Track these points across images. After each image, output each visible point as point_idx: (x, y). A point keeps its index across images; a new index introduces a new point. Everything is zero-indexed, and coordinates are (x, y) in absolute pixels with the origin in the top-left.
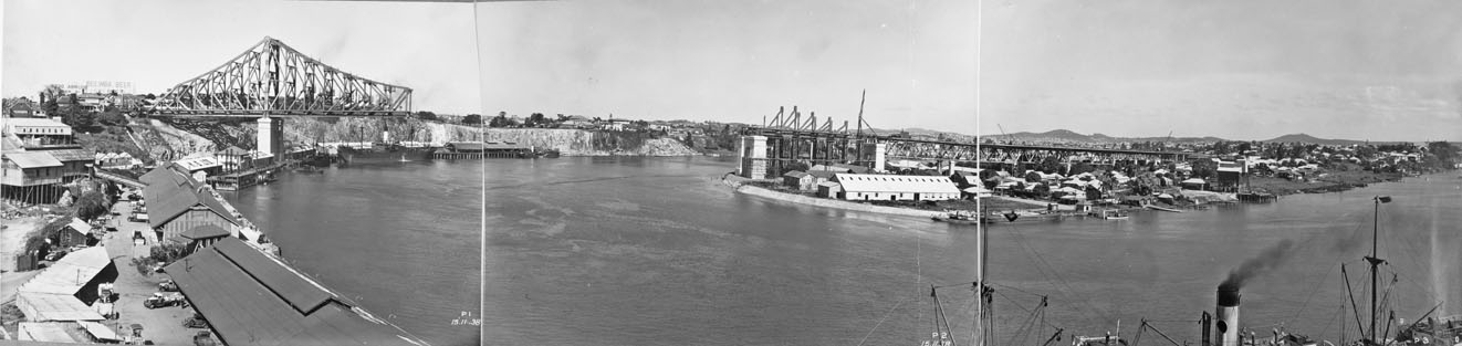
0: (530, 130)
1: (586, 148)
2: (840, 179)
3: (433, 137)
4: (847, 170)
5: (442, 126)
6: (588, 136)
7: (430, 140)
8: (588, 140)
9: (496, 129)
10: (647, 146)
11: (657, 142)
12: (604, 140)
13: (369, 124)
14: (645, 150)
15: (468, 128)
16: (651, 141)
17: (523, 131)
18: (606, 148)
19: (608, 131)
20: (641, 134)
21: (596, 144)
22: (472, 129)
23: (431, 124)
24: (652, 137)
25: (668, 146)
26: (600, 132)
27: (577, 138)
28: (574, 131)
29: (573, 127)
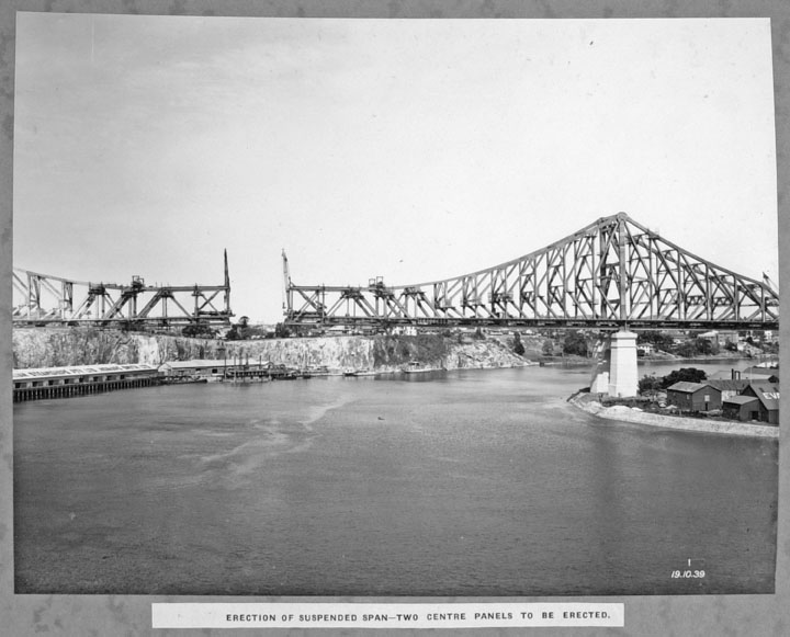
1: (365, 363)
2: (757, 392)
3: (141, 357)
4: (768, 377)
5: (153, 339)
6: (367, 345)
7: (136, 361)
8: (366, 353)
9: (236, 342)
10: (454, 356)
11: (470, 349)
13: (38, 340)
14: (451, 363)
16: (460, 349)
17: (274, 342)
18: (394, 361)
19: (396, 336)
20: (446, 339)
21: (379, 359)
24: (461, 342)
25: (486, 354)
26: (387, 338)
27: (351, 348)
28: (345, 340)
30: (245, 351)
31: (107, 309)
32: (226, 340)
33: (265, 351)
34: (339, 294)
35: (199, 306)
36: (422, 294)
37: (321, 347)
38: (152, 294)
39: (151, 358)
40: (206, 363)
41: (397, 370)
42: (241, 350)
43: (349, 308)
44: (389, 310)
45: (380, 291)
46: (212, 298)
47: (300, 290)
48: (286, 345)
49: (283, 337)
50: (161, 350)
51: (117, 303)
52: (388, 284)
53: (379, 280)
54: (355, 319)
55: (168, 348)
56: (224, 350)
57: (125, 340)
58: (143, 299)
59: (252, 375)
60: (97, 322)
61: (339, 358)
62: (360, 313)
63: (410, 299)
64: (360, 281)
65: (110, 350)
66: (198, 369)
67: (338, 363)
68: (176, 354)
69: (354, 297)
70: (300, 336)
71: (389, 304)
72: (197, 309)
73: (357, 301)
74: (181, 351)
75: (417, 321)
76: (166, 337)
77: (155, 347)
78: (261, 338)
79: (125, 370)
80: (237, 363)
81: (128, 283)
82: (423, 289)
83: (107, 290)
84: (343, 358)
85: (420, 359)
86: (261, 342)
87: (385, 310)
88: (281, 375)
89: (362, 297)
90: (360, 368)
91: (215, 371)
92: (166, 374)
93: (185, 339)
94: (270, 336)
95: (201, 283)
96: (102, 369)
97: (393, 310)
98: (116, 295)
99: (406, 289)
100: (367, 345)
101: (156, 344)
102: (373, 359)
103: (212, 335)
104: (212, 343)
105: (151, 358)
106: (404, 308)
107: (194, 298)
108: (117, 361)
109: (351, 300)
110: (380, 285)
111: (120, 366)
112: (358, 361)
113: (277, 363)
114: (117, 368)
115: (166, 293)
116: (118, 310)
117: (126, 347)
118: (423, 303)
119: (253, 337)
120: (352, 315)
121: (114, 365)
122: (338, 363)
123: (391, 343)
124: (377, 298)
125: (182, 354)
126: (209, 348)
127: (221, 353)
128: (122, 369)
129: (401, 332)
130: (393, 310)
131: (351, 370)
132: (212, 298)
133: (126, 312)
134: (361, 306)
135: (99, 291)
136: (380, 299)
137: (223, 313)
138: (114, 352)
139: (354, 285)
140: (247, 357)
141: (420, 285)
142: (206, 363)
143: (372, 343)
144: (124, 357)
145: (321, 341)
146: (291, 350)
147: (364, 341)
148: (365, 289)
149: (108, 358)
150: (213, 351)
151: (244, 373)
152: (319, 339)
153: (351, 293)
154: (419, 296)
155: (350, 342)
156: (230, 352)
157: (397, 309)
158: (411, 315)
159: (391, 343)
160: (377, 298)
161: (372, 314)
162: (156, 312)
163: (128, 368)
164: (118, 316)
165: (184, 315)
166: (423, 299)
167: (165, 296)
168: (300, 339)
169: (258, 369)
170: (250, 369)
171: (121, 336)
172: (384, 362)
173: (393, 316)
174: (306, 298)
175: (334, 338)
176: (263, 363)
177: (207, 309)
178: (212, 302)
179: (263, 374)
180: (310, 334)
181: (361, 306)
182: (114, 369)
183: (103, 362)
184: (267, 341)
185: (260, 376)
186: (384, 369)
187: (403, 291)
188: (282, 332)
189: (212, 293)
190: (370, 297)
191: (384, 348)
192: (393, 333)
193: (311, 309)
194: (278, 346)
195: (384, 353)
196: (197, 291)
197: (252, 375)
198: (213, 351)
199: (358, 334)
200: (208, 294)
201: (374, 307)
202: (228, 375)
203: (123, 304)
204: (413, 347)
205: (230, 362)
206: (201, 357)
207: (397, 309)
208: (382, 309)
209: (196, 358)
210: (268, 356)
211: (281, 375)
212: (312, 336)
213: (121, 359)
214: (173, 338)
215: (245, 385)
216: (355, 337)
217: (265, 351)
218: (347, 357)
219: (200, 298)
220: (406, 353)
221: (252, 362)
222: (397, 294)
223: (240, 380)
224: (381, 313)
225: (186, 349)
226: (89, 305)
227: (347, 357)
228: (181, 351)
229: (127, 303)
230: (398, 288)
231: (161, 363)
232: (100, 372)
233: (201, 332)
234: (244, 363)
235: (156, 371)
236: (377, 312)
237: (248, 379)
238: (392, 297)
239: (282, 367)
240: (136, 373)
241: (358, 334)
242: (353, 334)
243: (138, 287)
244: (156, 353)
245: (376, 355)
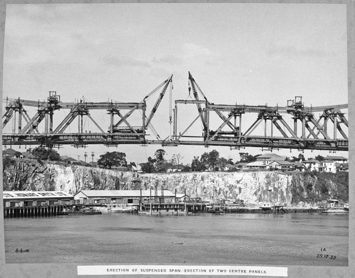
0: (199, 175)
1: (283, 199)
3: (57, 185)
5: (69, 169)
6: (285, 180)
7: (52, 189)
8: (284, 190)
9: (151, 175)
12: (309, 187)
15: (107, 172)
17: (190, 175)
18: (311, 199)
19: (315, 172)
21: (297, 197)
22: (113, 173)
23: (51, 166)
26: (305, 174)
27: (268, 184)
28: (262, 175)
29: (263, 168)
30: (161, 183)
31: (24, 124)
32: (142, 173)
33: (181, 184)
34: (256, 115)
35: (115, 124)
36: (341, 115)
37: (238, 182)
38: (68, 111)
39: (67, 187)
40: (121, 193)
41: (316, 207)
42: (157, 183)
43: (264, 129)
44: (307, 133)
45: (299, 112)
46: (128, 116)
47: (218, 109)
48: (202, 179)
49: (199, 170)
50: (77, 180)
51: (34, 119)
52: (306, 104)
53: (298, 100)
54: (273, 140)
55: (84, 178)
56: (140, 182)
57: (42, 169)
58: (60, 115)
59: (168, 207)
60: (13, 137)
61: (256, 194)
62: (277, 134)
63: (329, 121)
64: (279, 100)
65: (26, 178)
66: (114, 198)
67: (255, 198)
68: (92, 184)
69: (271, 117)
70: (217, 170)
71: (307, 126)
72: (113, 126)
73: (274, 122)
74: (97, 182)
75: (335, 143)
76: (81, 167)
77: (71, 177)
78: (177, 172)
79: (41, 196)
80: (153, 194)
81: (44, 98)
82: (342, 111)
83: (25, 107)
84: (260, 194)
85: (339, 197)
86: (177, 175)
87: (303, 134)
88: (196, 209)
89: (280, 118)
90: (277, 204)
91: (130, 201)
92: (82, 202)
93: (101, 170)
94: (186, 169)
95: (116, 99)
96: (18, 195)
97: (312, 132)
98: (32, 112)
99: (326, 111)
100: (285, 180)
101: (72, 175)
102: (290, 195)
103: (129, 167)
104: (128, 174)
105: (67, 187)
106: (323, 130)
107: (110, 116)
108: (34, 189)
109: (269, 122)
110: (299, 106)
111: (36, 193)
112: (275, 197)
113: (193, 196)
114: (33, 195)
115: (82, 110)
116: (34, 127)
117: (42, 175)
118: (342, 125)
119: (169, 170)
120: (269, 135)
121: (31, 192)
122: (255, 198)
123: (310, 180)
124: (295, 121)
125: (97, 183)
126: (125, 180)
127: (136, 184)
128: (38, 195)
129: (321, 169)
130: (312, 132)
131: (269, 205)
132: (128, 116)
133: (42, 129)
134: (279, 128)
135: (18, 106)
136: (298, 121)
137: (138, 131)
138: (30, 180)
139: (272, 104)
140: (163, 189)
141: (340, 107)
142: (121, 193)
143: (290, 178)
144: (40, 185)
145: (238, 175)
146: (207, 183)
147: (282, 176)
148: (282, 108)
149: (24, 186)
150: (129, 183)
151: (160, 205)
152: (235, 173)
153: (266, 113)
154: (338, 119)
155: (267, 177)
156: (145, 185)
157: (316, 131)
158: (331, 136)
159: (310, 180)
160: (295, 121)
161: (290, 136)
162: (73, 129)
163: (44, 194)
164: (34, 133)
165: (99, 132)
166: (343, 121)
167: (80, 113)
168: (217, 173)
169: (173, 202)
170: (166, 201)
171: (37, 164)
172: (303, 199)
173: (312, 137)
174: (223, 118)
175: (251, 173)
176: (178, 196)
177: (123, 126)
178: (128, 119)
179: (178, 207)
180: (227, 169)
181: (279, 128)
182: (30, 195)
183: (20, 189)
184: (183, 175)
185: (176, 210)
186: (300, 206)
187: (322, 113)
188: (197, 166)
189: (127, 111)
190: (288, 118)
191: (302, 184)
192: (312, 169)
193: (227, 129)
194: (194, 179)
195: (302, 190)
196: (113, 109)
197: (168, 207)
198: (129, 183)
199: (276, 169)
200: (123, 112)
201: (293, 128)
202: (143, 206)
203: (40, 121)
204: (332, 184)
205: (146, 193)
206: (117, 188)
207: (316, 131)
208: (301, 131)
209: (111, 189)
210: (184, 190)
211: (196, 209)
212: (229, 171)
213: (37, 187)
214: (89, 168)
215: (161, 216)
216: (273, 172)
217: (181, 184)
218: (264, 192)
219: (116, 116)
220: (324, 190)
221: (167, 193)
222: (317, 115)
223: (155, 212)
224: (299, 135)
225: (102, 180)
226: (6, 122)
227: (264, 192)
228: (97, 182)
229: (43, 121)
230: (318, 109)
231: (77, 192)
232: (16, 197)
233: (117, 164)
234: (159, 194)
235: (72, 198)
236: (295, 133)
237: (163, 212)
238: (311, 117)
239: (198, 200)
240: (52, 200)
241: (276, 169)
242: (271, 169)
243: (54, 104)
244: (71, 182)
245: (294, 191)
